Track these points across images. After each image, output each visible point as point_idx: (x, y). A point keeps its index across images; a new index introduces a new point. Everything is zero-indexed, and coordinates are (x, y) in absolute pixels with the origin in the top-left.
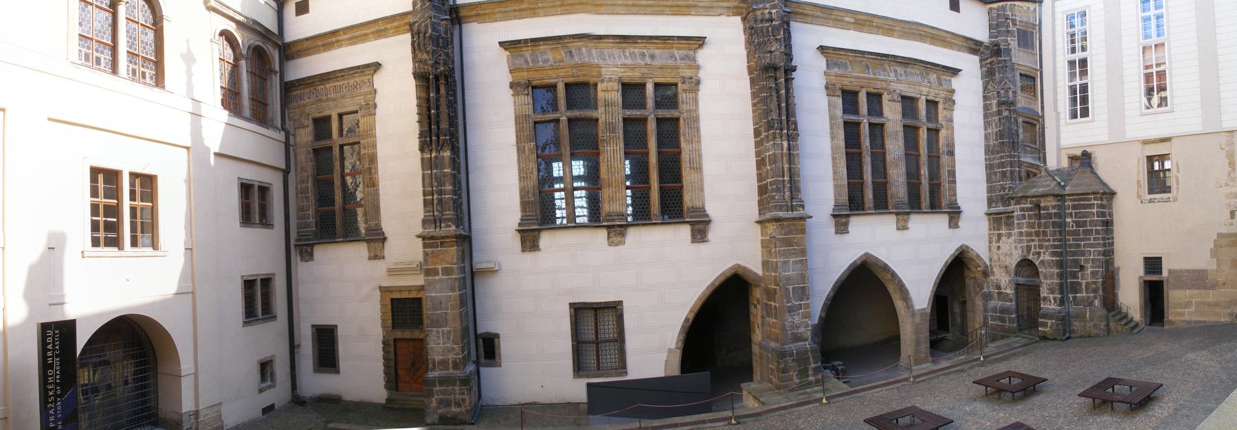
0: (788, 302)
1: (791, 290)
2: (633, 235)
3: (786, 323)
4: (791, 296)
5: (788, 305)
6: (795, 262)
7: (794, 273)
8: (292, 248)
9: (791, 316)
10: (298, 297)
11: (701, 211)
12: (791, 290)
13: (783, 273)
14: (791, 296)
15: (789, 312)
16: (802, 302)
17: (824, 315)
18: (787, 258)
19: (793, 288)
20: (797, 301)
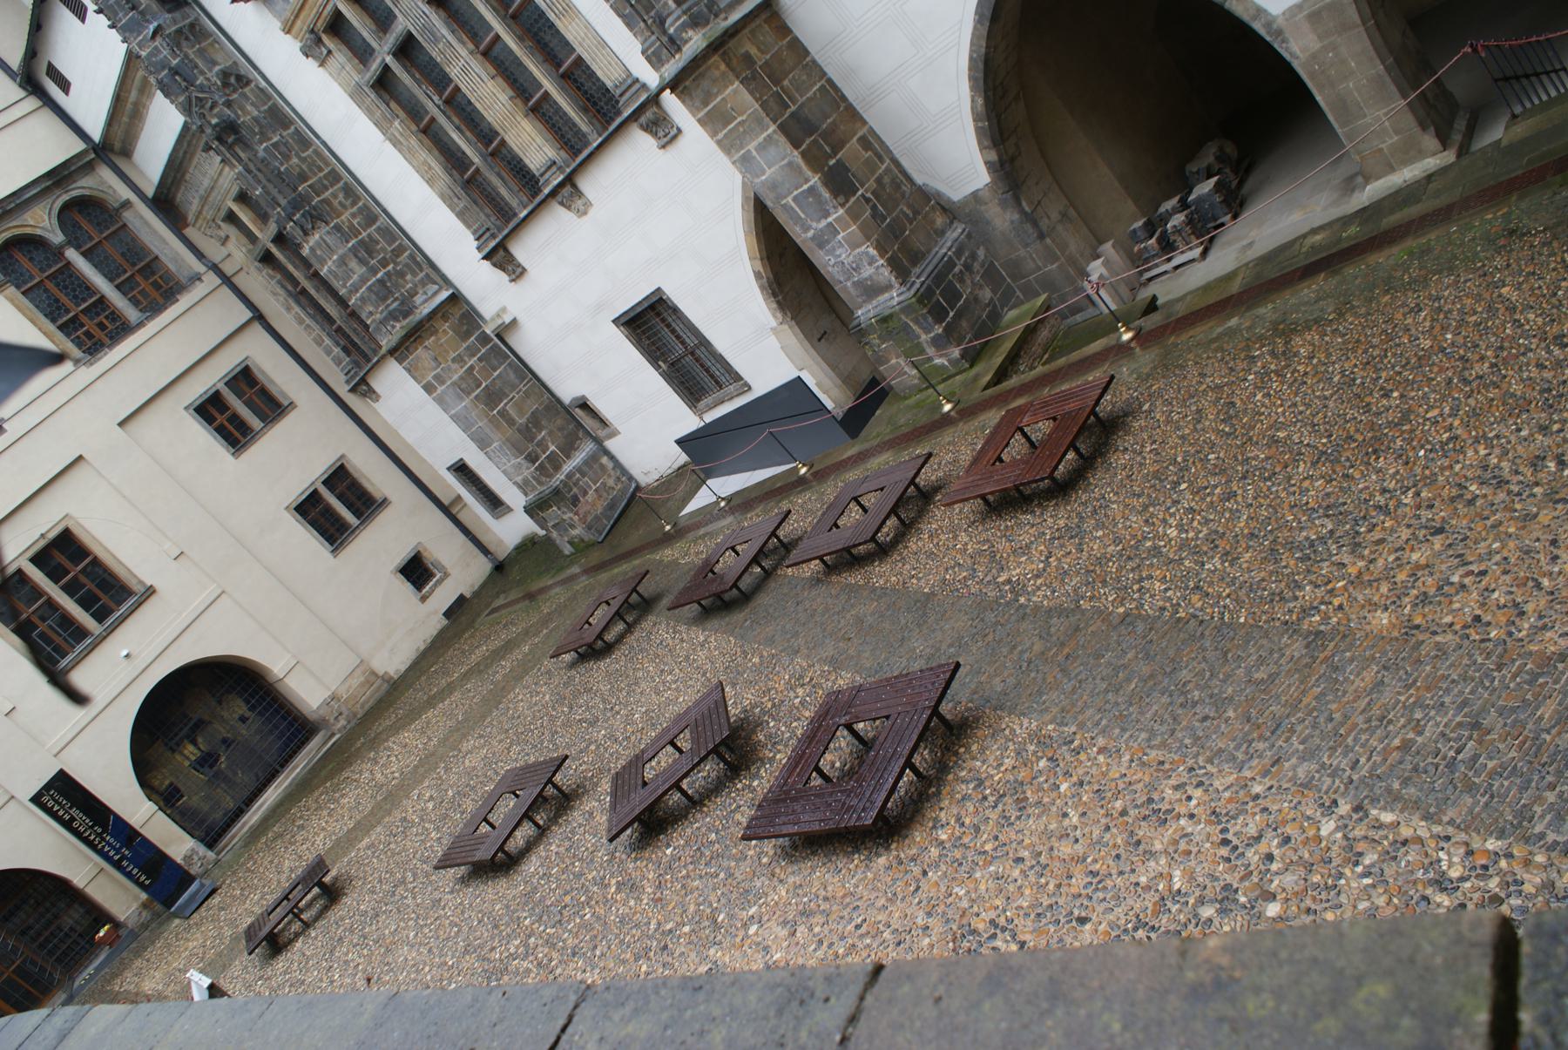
0: (806, 229)
1: (793, 205)
2: (590, 184)
3: (830, 269)
4: (803, 216)
5: (810, 234)
6: (760, 148)
7: (773, 169)
8: (353, 401)
9: (831, 252)
10: (408, 446)
11: (630, 86)
12: (793, 205)
13: (757, 181)
14: (803, 216)
15: (821, 246)
16: (830, 219)
17: (993, 156)
18: (742, 147)
19: (795, 199)
20: (819, 221)
